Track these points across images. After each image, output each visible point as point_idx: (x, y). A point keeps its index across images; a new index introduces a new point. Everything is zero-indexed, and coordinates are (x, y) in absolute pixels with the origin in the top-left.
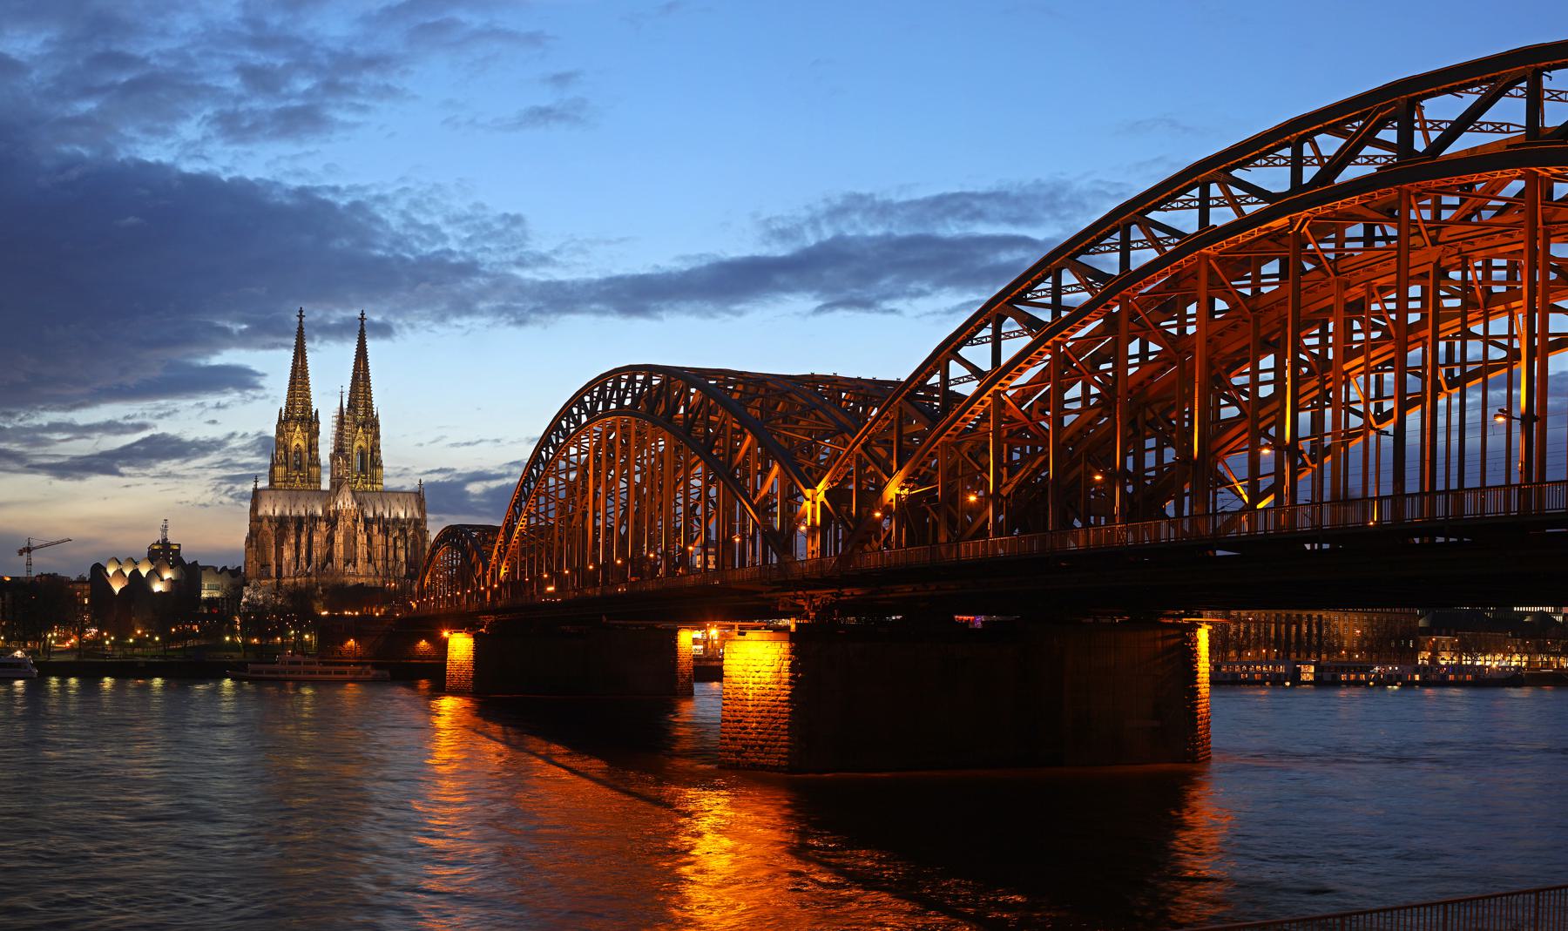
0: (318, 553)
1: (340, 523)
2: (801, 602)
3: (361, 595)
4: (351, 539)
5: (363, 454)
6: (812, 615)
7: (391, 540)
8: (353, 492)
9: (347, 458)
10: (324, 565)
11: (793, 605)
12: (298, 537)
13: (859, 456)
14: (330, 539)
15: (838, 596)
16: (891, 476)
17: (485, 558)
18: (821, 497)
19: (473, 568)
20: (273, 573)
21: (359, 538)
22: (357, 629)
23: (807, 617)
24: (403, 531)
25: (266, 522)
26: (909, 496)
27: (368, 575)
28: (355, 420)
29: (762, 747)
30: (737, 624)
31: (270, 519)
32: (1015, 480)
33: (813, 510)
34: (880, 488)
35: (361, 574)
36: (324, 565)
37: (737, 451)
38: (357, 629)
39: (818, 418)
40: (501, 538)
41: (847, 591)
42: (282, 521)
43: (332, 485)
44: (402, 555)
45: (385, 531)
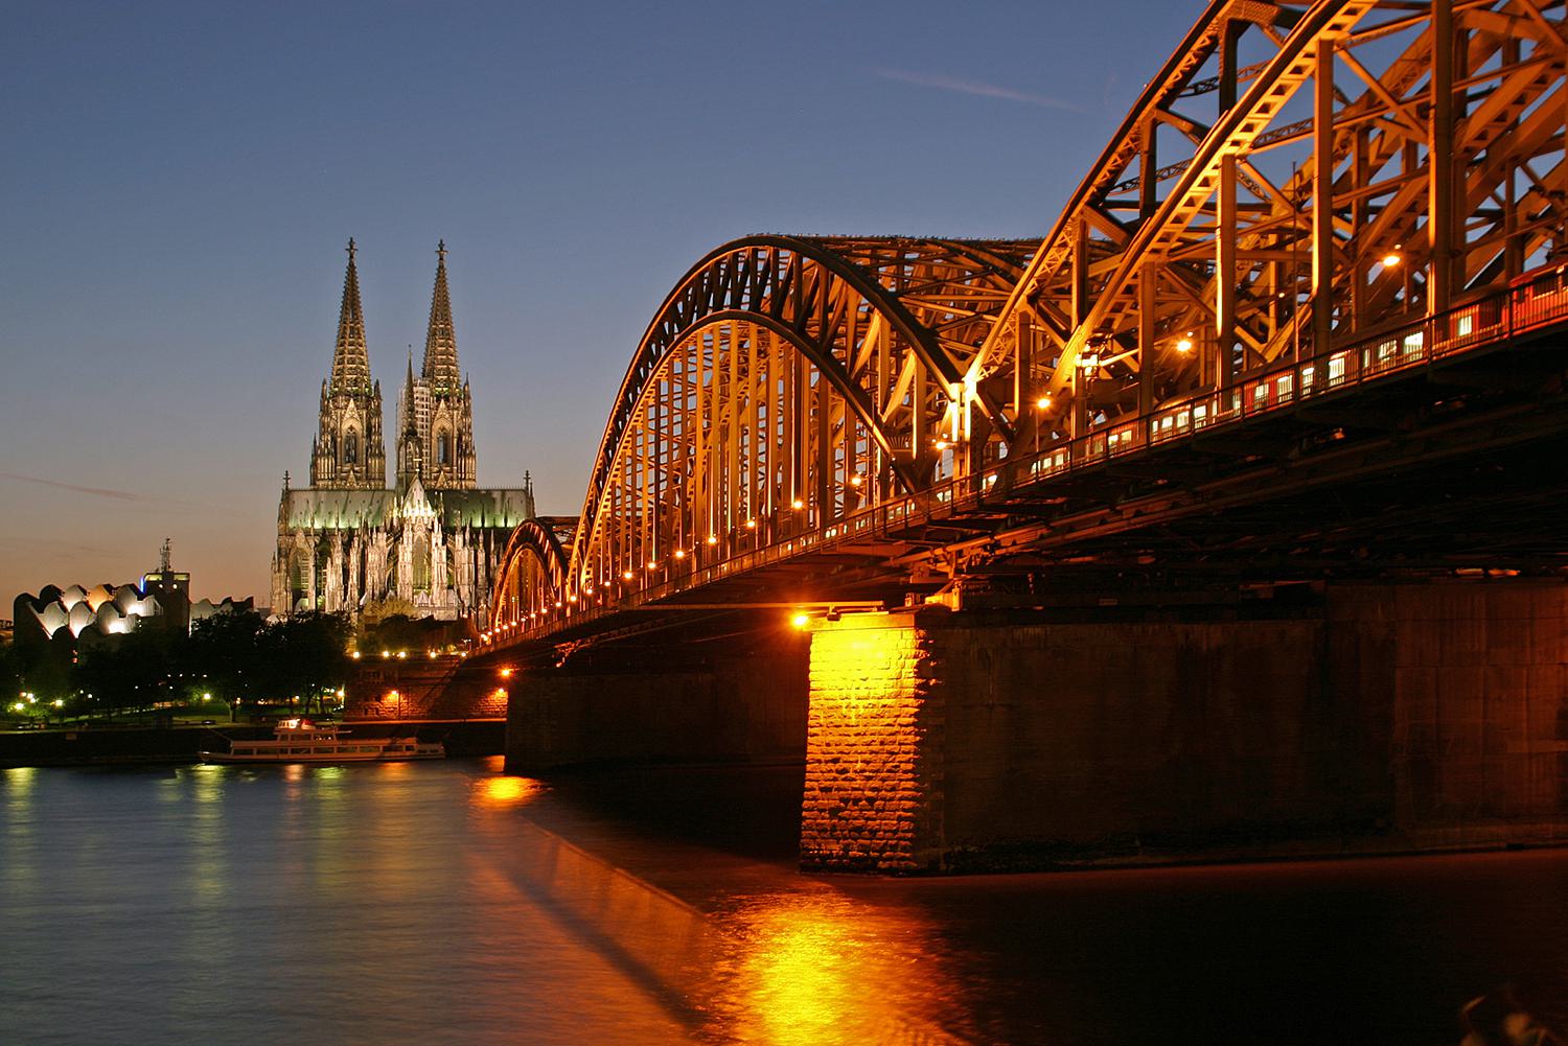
1: (407, 534)
2: (942, 567)
3: (431, 629)
4: (422, 557)
5: (445, 438)
7: (482, 556)
10: (383, 595)
11: (935, 573)
13: (1024, 316)
14: (393, 556)
17: (564, 561)
21: (435, 555)
25: (300, 536)
27: (448, 607)
29: (871, 801)
31: (307, 533)
35: (437, 603)
36: (383, 595)
38: (400, 676)
40: (581, 529)
41: (1004, 537)
42: (325, 536)
43: (400, 481)
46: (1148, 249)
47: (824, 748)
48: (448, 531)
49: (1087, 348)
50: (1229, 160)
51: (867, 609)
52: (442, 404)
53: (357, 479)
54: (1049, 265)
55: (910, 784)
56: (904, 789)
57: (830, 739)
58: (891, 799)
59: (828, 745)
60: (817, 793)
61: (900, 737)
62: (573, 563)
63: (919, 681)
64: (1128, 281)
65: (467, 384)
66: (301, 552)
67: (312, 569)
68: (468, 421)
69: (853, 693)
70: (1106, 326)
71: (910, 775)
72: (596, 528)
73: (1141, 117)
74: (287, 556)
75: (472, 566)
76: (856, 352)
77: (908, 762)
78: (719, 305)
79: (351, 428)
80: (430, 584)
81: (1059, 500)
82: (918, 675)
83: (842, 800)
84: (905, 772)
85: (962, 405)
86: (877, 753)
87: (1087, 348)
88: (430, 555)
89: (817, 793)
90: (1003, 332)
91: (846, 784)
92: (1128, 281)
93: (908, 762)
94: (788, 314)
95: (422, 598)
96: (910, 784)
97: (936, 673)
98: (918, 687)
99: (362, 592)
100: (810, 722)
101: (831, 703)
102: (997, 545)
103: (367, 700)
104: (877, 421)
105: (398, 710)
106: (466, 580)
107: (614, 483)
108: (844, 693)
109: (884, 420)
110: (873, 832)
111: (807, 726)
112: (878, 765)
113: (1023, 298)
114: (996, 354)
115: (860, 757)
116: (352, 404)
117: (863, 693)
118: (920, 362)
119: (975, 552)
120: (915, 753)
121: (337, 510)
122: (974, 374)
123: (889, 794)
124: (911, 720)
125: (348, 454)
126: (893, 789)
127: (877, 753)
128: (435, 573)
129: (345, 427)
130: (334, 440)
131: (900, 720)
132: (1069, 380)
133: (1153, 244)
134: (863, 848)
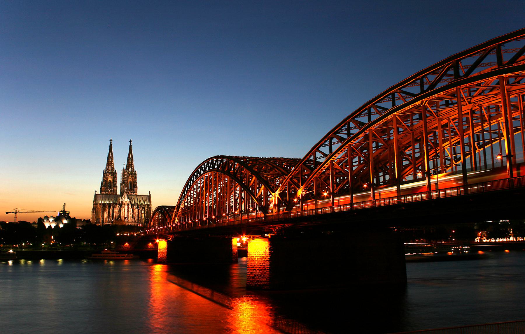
0: (116, 215)
1: (123, 205)
2: (272, 228)
3: (131, 228)
5: (131, 183)
6: (275, 232)
8: (128, 195)
12: (109, 210)
13: (289, 182)
14: (120, 211)
15: (284, 226)
16: (299, 188)
17: (170, 217)
18: (277, 195)
19: (166, 220)
21: (129, 210)
22: (129, 239)
23: (274, 233)
24: (144, 208)
25: (99, 205)
26: (305, 194)
30: (251, 236)
31: (100, 204)
32: (339, 188)
33: (275, 199)
34: (296, 192)
35: (130, 221)
36: (118, 219)
37: (250, 182)
39: (276, 171)
40: (175, 210)
41: (286, 225)
42: (104, 205)
43: (121, 193)
44: (143, 215)
45: (138, 208)
50: (332, 161)
66: (99, 209)
95: (126, 220)
105: (126, 247)
110: (261, 281)
121: (107, 199)
122: (278, 192)
134: (259, 285)
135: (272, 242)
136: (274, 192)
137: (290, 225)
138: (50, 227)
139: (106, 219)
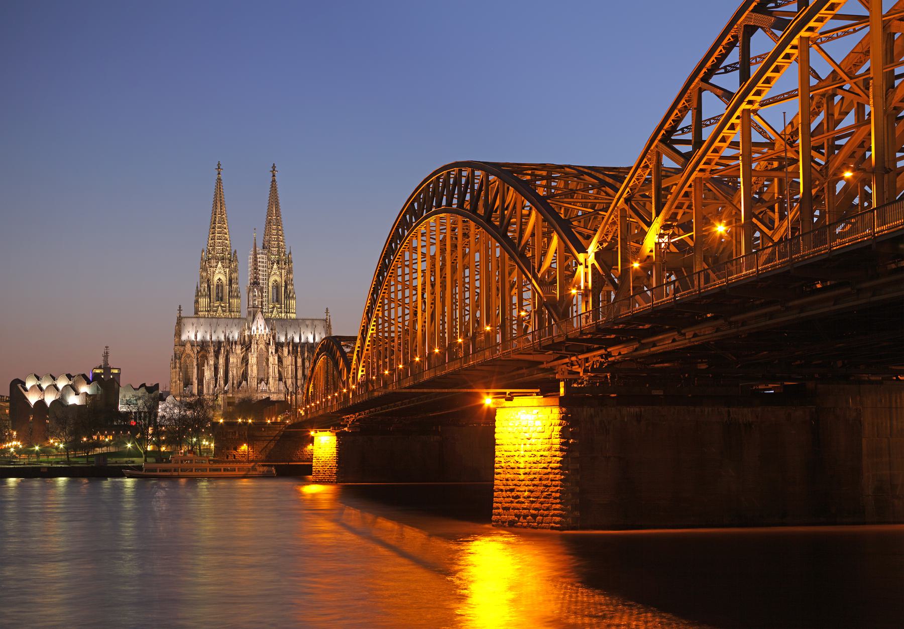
0: (234, 372)
2: (576, 368)
4: (263, 361)
5: (277, 287)
7: (299, 361)
9: (261, 290)
11: (571, 372)
14: (245, 360)
16: (649, 224)
17: (348, 363)
18: (592, 260)
19: (340, 373)
20: (195, 391)
21: (271, 359)
25: (188, 346)
26: (668, 245)
27: (279, 392)
28: (269, 259)
29: (534, 516)
33: (586, 274)
35: (273, 390)
38: (251, 435)
40: (358, 343)
42: (203, 346)
43: (249, 313)
46: (698, 169)
47: (505, 482)
48: (279, 346)
49: (662, 231)
51: (530, 394)
52: (275, 266)
53: (224, 311)
54: (638, 179)
55: (558, 506)
56: (555, 509)
57: (508, 476)
58: (547, 515)
59: (507, 480)
60: (501, 511)
61: (551, 476)
62: (353, 366)
63: (562, 440)
64: (686, 189)
65: (290, 253)
66: (189, 356)
67: (196, 367)
68: (291, 276)
69: (522, 448)
70: (673, 217)
71: (558, 501)
72: (367, 343)
73: (692, 86)
74: (180, 358)
75: (294, 367)
76: (522, 232)
77: (557, 492)
78: (439, 204)
79: (219, 279)
80: (268, 378)
81: (647, 326)
82: (562, 437)
83: (516, 515)
84: (555, 498)
85: (587, 267)
86: (537, 486)
87: (662, 231)
88: (268, 359)
89: (501, 511)
90: (610, 221)
91: (518, 505)
92: (686, 189)
93: (557, 492)
94: (481, 211)
95: (263, 386)
96: (558, 506)
97: (573, 435)
98: (562, 444)
99: (226, 382)
100: (496, 465)
101: (509, 454)
102: (609, 355)
103: (228, 449)
104: (535, 276)
106: (290, 376)
107: (377, 315)
108: (517, 447)
109: (539, 276)
111: (494, 468)
112: (538, 494)
113: (622, 199)
114: (607, 235)
115: (527, 488)
116: (220, 265)
117: (528, 447)
118: (562, 243)
119: (595, 359)
120: (561, 486)
122: (593, 248)
123: (546, 513)
124: (558, 465)
125: (217, 295)
126: (548, 509)
127: (537, 486)
128: (271, 370)
129: (216, 279)
130: (209, 286)
131: (551, 465)
132: (651, 251)
133: (701, 166)
135: (571, 408)
136: (583, 250)
137: (624, 351)
138: (41, 403)
139: (209, 384)
